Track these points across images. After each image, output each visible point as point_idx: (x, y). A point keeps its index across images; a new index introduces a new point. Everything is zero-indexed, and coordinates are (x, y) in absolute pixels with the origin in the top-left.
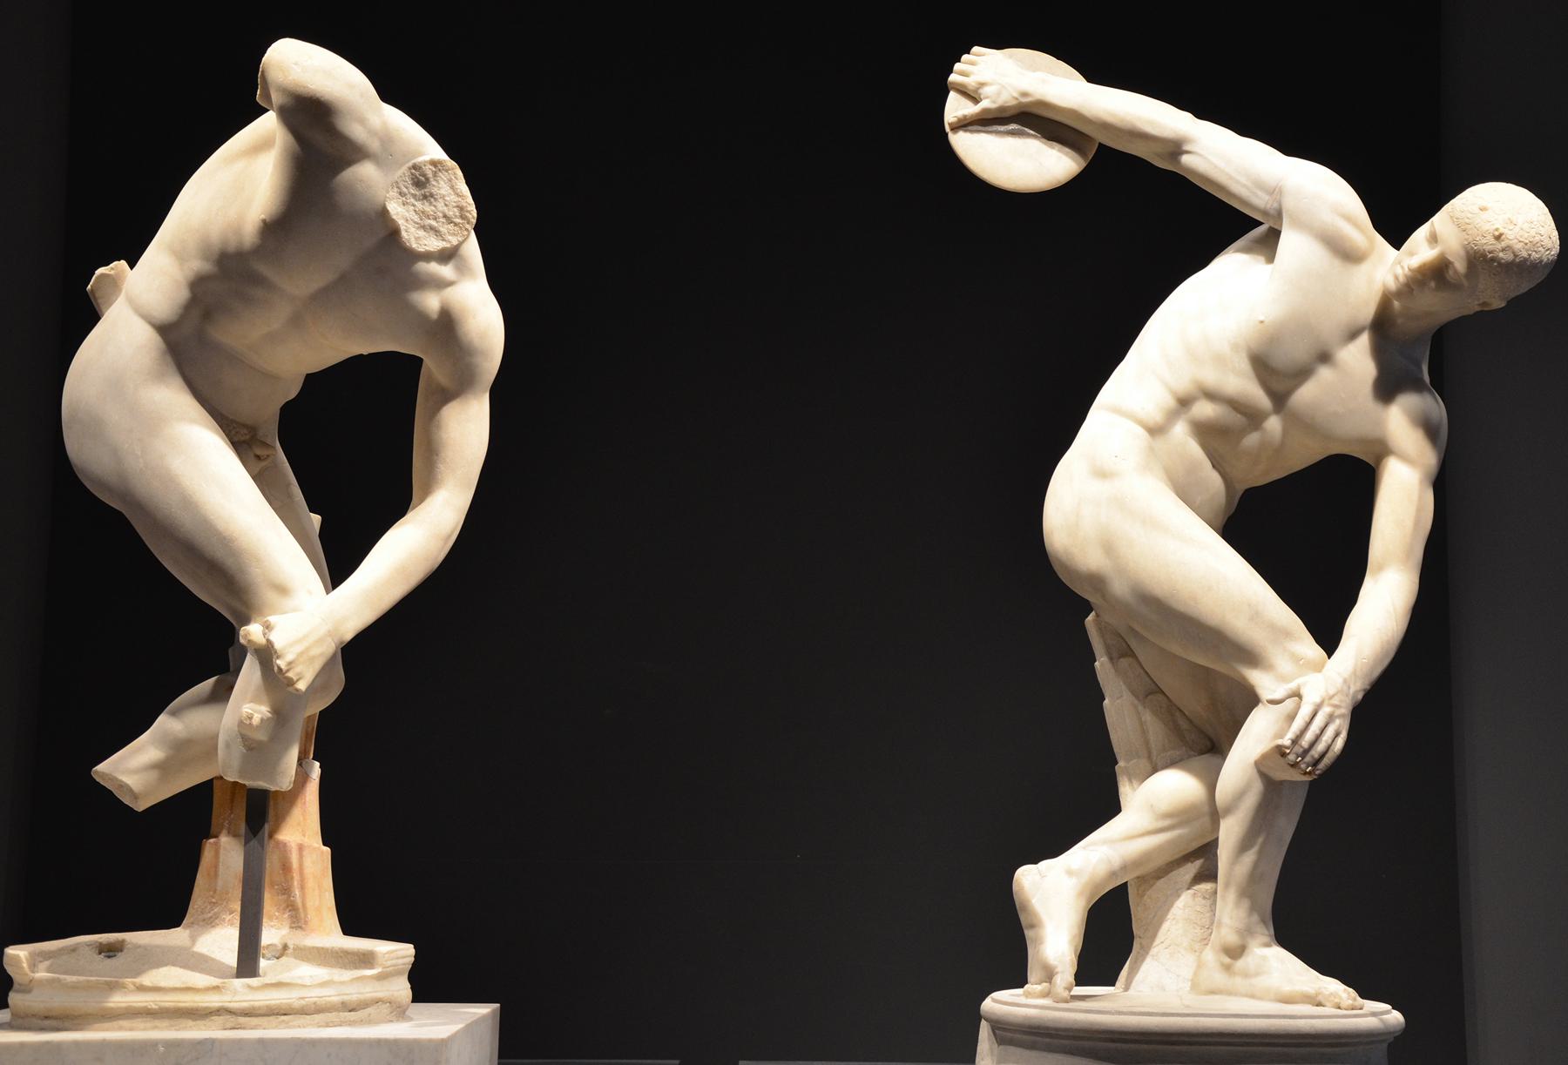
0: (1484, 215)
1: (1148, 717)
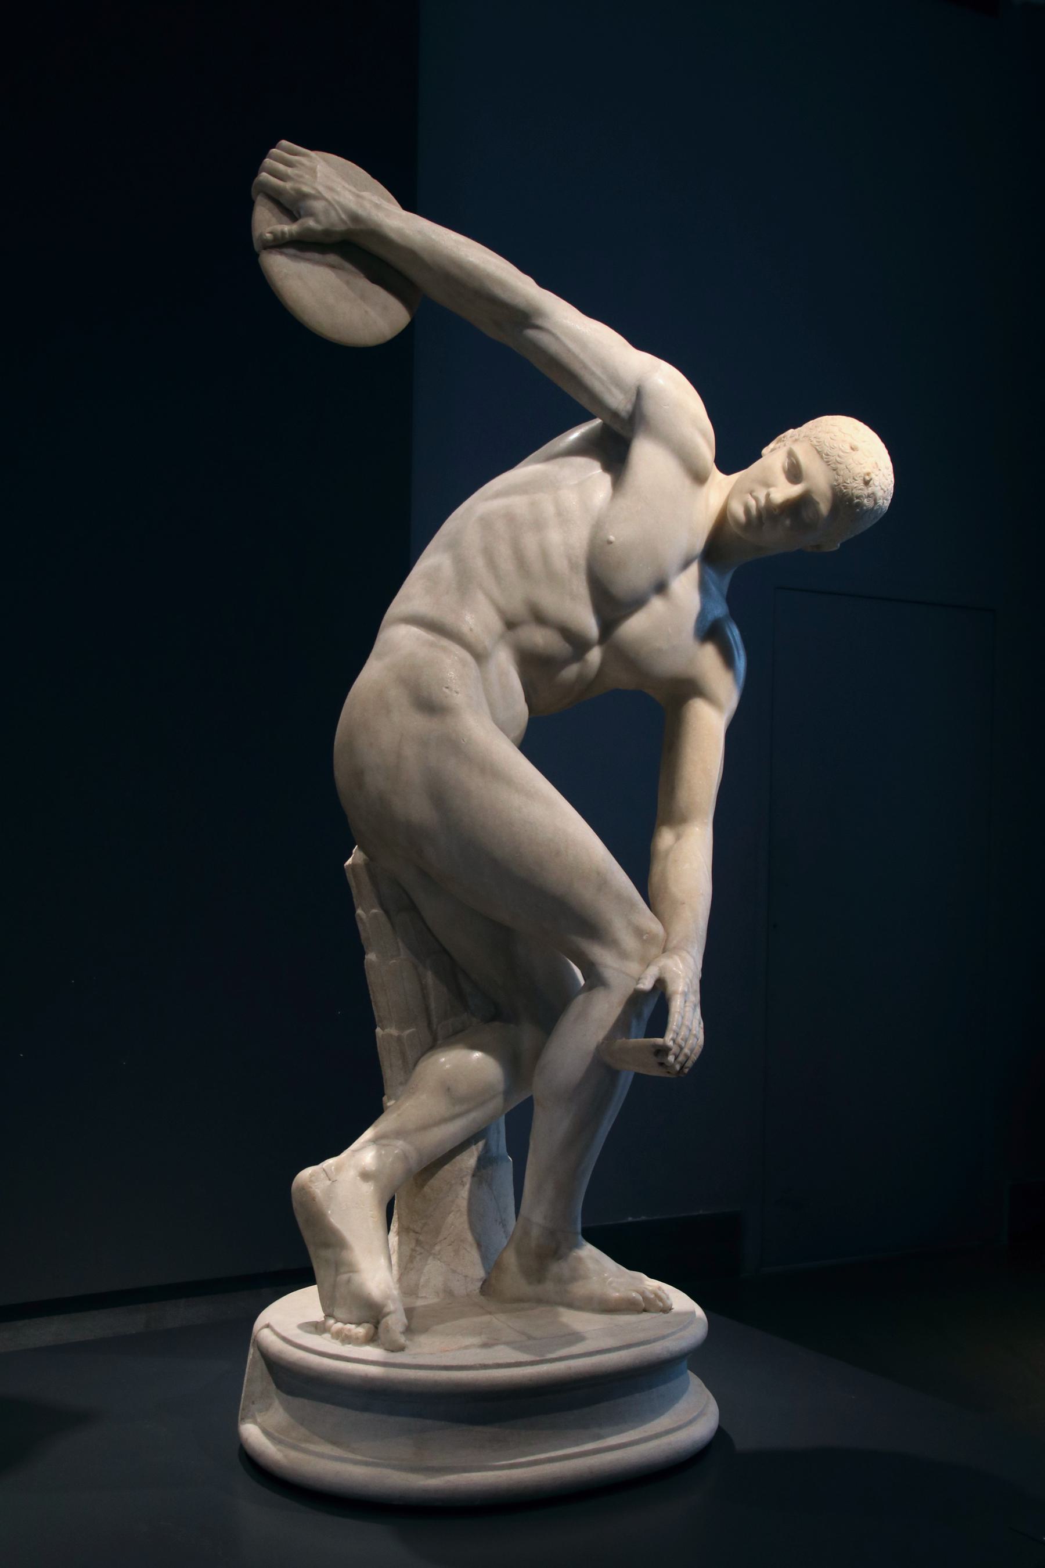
0: (856, 456)
1: (430, 978)
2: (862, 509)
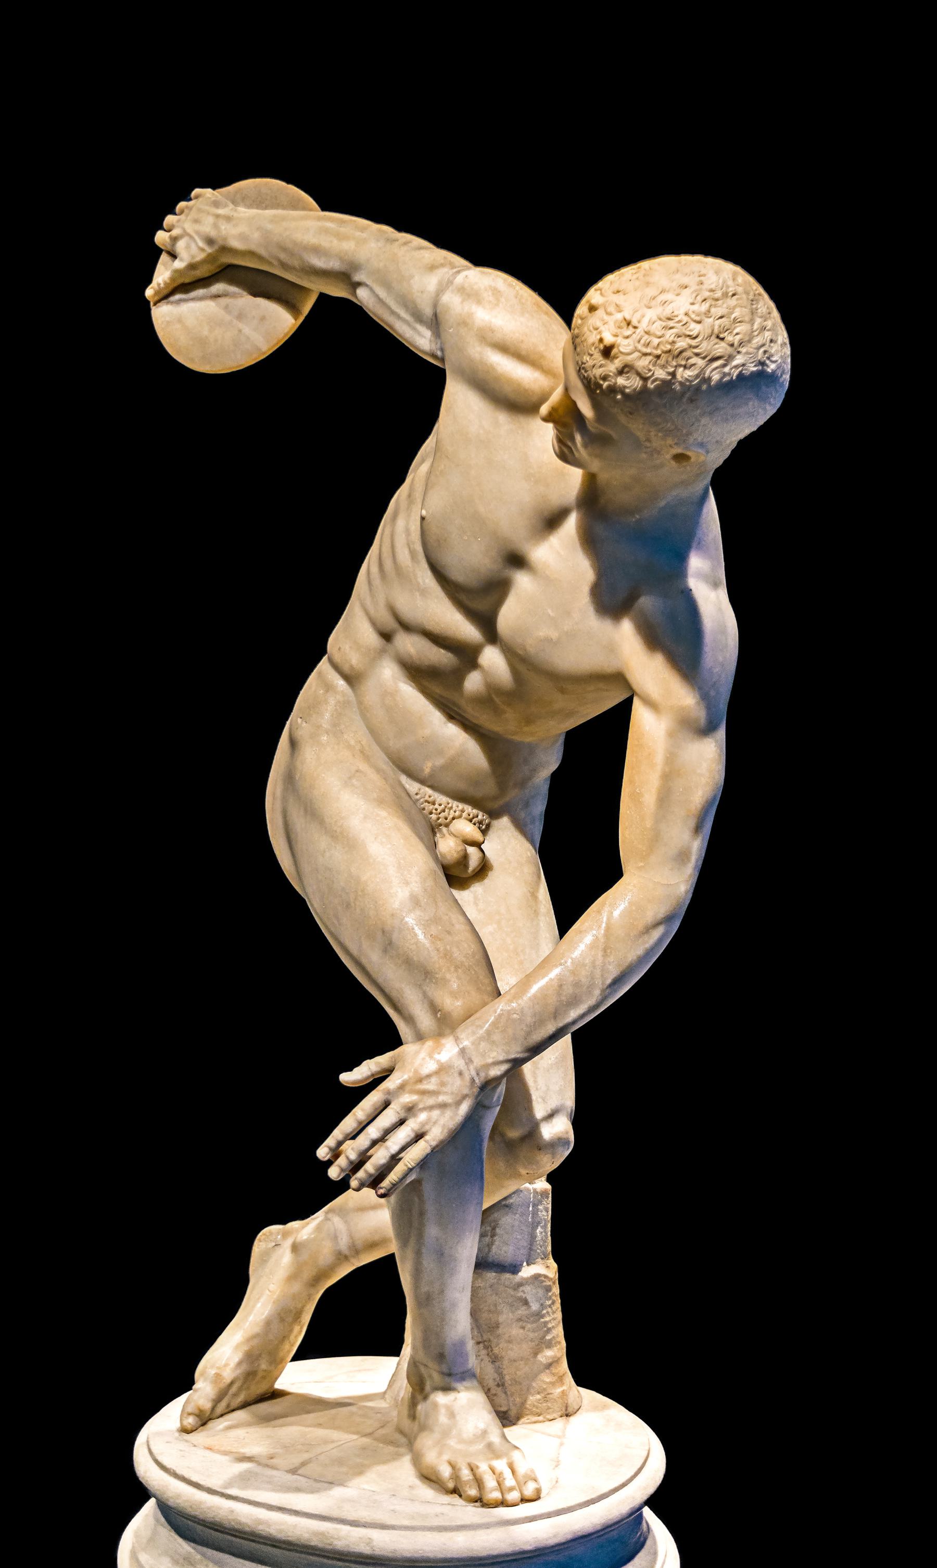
2: (623, 393)
